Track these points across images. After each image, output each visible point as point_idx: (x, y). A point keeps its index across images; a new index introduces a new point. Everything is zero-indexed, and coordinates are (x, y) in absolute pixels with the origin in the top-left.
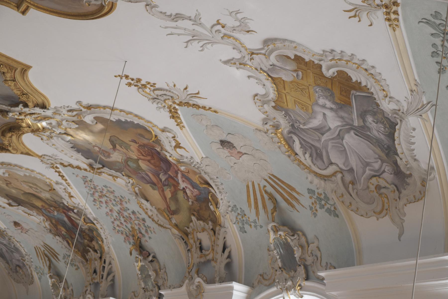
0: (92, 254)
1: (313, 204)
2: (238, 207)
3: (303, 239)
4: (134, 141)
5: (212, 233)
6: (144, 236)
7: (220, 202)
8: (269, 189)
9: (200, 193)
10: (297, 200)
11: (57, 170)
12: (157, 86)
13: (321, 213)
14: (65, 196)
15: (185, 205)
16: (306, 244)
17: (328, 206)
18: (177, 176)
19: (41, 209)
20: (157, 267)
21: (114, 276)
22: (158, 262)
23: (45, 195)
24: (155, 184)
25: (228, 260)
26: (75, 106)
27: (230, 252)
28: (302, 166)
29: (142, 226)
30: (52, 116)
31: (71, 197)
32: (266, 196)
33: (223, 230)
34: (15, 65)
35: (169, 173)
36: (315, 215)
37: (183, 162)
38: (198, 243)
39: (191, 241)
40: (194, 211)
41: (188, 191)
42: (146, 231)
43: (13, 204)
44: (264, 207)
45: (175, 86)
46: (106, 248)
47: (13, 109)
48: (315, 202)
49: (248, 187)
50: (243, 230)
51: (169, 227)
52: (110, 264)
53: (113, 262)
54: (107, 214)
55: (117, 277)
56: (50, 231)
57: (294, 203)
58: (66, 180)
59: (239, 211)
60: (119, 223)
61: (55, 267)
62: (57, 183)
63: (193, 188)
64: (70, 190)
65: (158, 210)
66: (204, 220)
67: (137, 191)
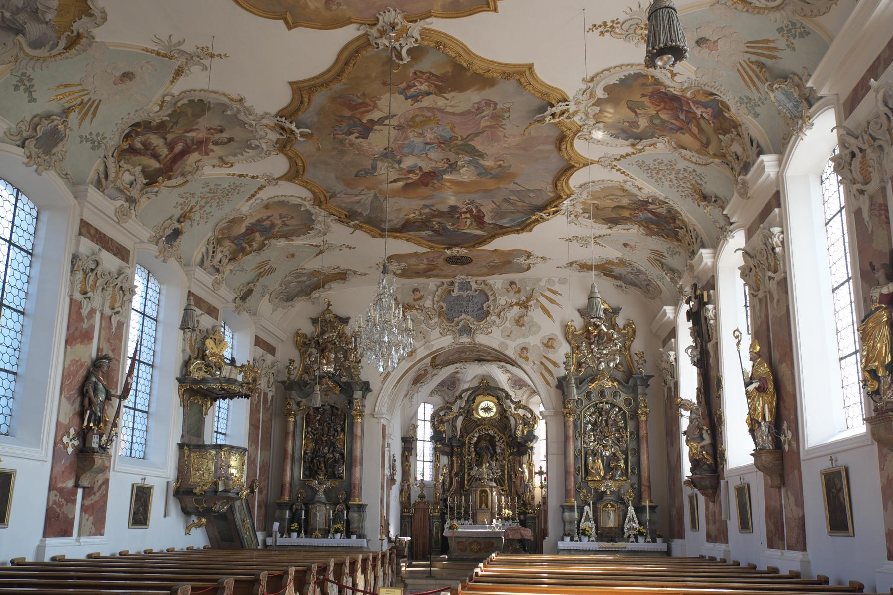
0: (681, 232)
1: (787, 40)
2: (743, 97)
3: (796, 78)
4: (644, 95)
5: (738, 138)
6: (701, 185)
7: (729, 103)
8: (754, 58)
9: (713, 109)
10: (775, 48)
11: (617, 168)
12: (621, 21)
13: (797, 42)
14: (635, 191)
15: (709, 128)
16: (800, 81)
17: (798, 30)
18: (690, 107)
19: (630, 218)
20: (722, 204)
21: (701, 238)
22: (720, 198)
23: (625, 201)
24: (681, 129)
25: (758, 149)
26: (584, 87)
27: (757, 143)
28: (761, 11)
29: (697, 177)
30: (577, 109)
31: (640, 189)
32: (754, 67)
33: (743, 127)
34: (521, 69)
35: (684, 108)
36: (794, 49)
37: (685, 89)
38: (734, 156)
39: (729, 158)
40: (719, 130)
41: (705, 115)
42: (701, 180)
43: (612, 225)
44: (759, 79)
45: (631, 10)
46: (686, 219)
47: (545, 113)
48: (788, 36)
49: (738, 71)
50: (756, 115)
51: (711, 160)
52: (694, 230)
53: (696, 228)
54: (670, 187)
55: (704, 239)
56: (647, 234)
57: (775, 53)
58: (628, 174)
59: (746, 101)
60: (681, 189)
61: (666, 265)
62: (625, 182)
63: (706, 108)
64: (636, 183)
65: (697, 151)
66: (729, 132)
67: (675, 146)
